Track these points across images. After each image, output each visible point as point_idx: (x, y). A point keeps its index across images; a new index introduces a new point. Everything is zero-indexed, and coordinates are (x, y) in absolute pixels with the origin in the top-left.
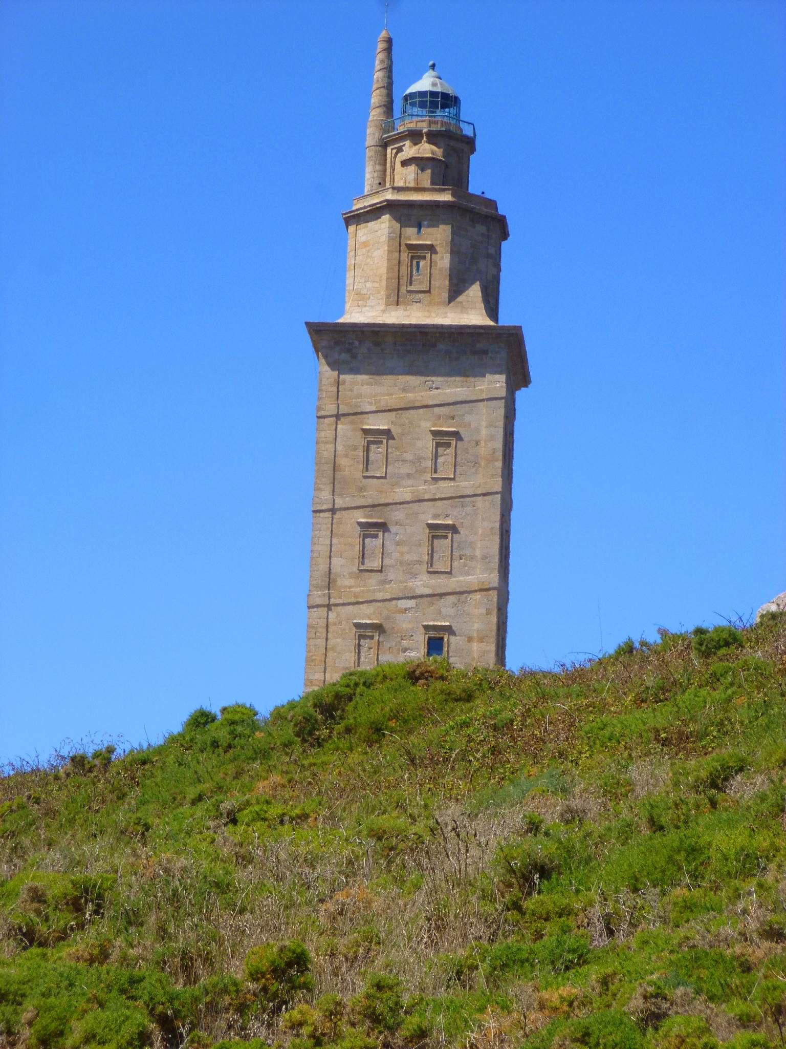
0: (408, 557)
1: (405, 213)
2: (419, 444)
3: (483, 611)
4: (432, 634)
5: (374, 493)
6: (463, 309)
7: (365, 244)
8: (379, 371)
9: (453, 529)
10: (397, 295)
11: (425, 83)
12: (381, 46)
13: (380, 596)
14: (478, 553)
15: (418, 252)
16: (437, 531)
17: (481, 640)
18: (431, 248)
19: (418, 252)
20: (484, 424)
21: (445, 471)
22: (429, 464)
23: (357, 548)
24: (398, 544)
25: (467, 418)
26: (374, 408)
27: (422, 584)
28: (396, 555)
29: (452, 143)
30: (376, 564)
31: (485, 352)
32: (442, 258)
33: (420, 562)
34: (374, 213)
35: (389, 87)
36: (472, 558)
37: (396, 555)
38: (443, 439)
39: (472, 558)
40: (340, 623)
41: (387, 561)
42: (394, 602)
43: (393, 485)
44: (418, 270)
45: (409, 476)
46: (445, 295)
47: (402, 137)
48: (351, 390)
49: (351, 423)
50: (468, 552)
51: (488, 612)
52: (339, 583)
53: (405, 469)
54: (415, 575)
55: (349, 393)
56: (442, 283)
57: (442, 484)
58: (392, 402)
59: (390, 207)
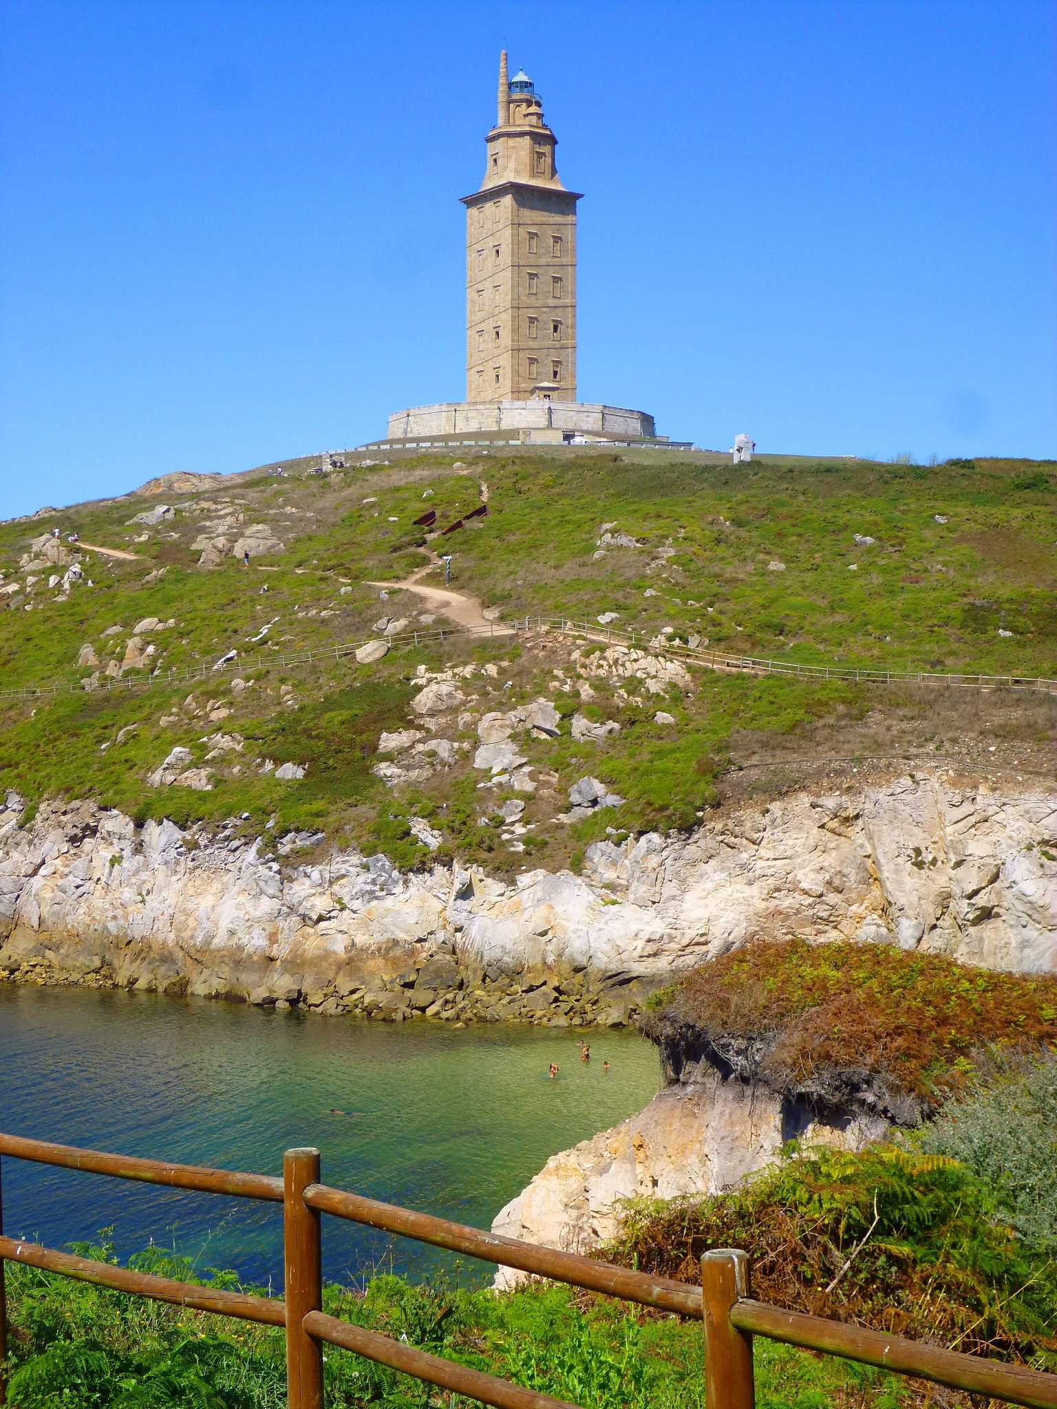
1: (537, 138)
5: (532, 261)
6: (556, 183)
7: (514, 148)
8: (532, 208)
9: (560, 279)
10: (534, 173)
11: (521, 77)
12: (503, 57)
15: (540, 155)
16: (556, 280)
18: (544, 154)
19: (540, 155)
27: (551, 302)
34: (522, 134)
38: (557, 239)
47: (522, 101)
53: (542, 251)
56: (548, 171)
59: (530, 134)
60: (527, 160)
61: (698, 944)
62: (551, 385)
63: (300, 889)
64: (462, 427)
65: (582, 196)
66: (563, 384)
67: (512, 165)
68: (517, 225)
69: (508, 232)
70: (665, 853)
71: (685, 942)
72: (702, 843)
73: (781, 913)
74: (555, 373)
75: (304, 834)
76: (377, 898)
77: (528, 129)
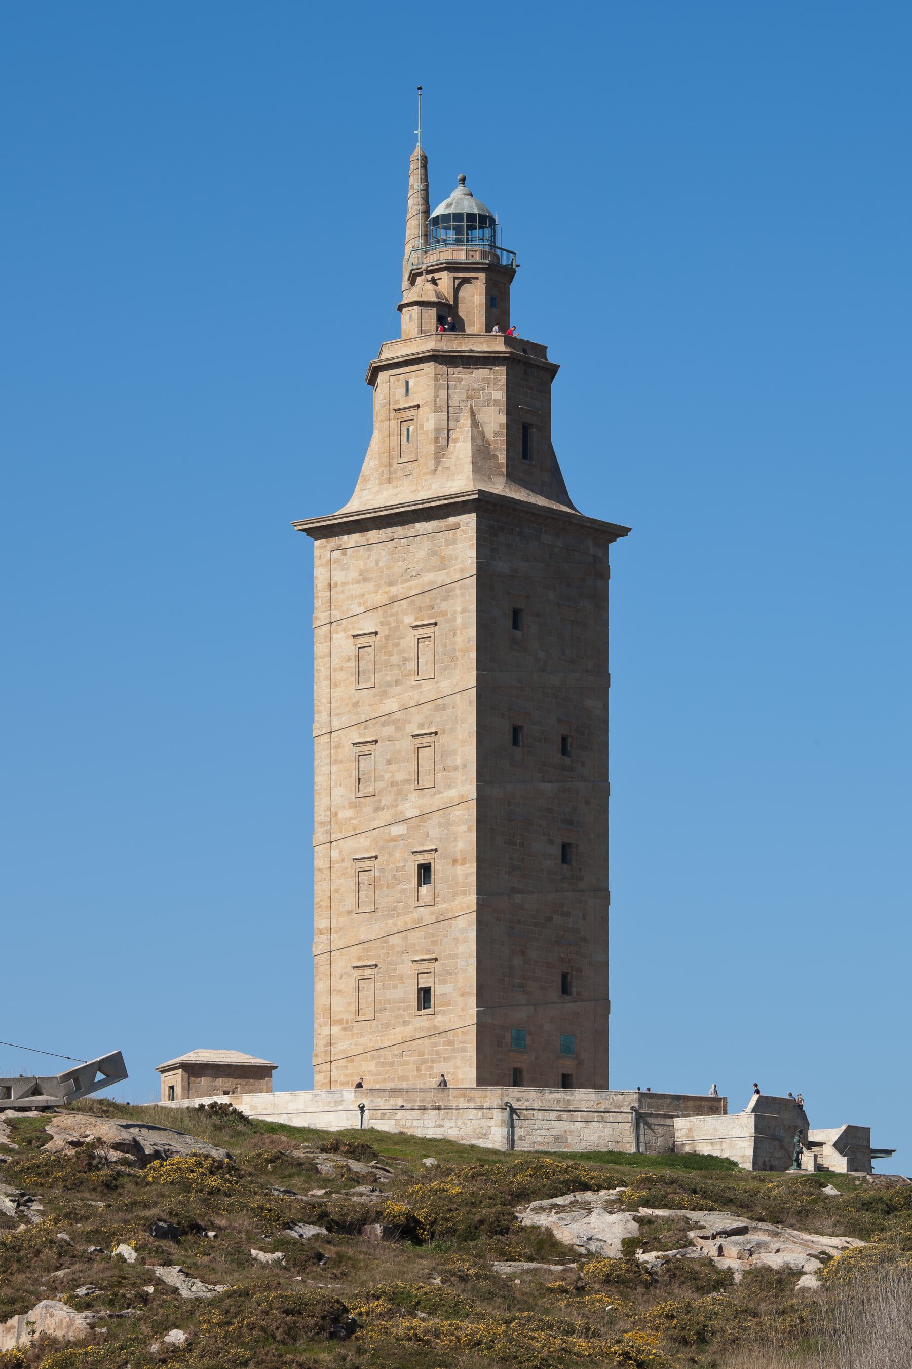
0: (400, 776)
2: (404, 643)
3: (465, 828)
4: (422, 859)
13: (375, 824)
14: (459, 762)
17: (464, 862)
20: (459, 609)
21: (426, 669)
22: (411, 665)
23: (355, 774)
24: (389, 762)
25: (444, 606)
26: (362, 609)
27: (411, 806)
28: (387, 776)
29: (461, 275)
30: (371, 790)
31: (456, 527)
32: (428, 420)
33: (408, 781)
35: (427, 212)
36: (455, 768)
37: (387, 776)
39: (455, 768)
40: (343, 860)
41: (380, 785)
42: (387, 829)
43: (384, 694)
44: (408, 440)
45: (397, 682)
46: (431, 464)
48: (343, 592)
49: (345, 630)
50: (449, 762)
51: (469, 830)
52: (340, 816)
54: (405, 798)
55: (342, 596)
57: (427, 686)
58: (379, 598)
66: (441, 1021)
74: (425, 996)
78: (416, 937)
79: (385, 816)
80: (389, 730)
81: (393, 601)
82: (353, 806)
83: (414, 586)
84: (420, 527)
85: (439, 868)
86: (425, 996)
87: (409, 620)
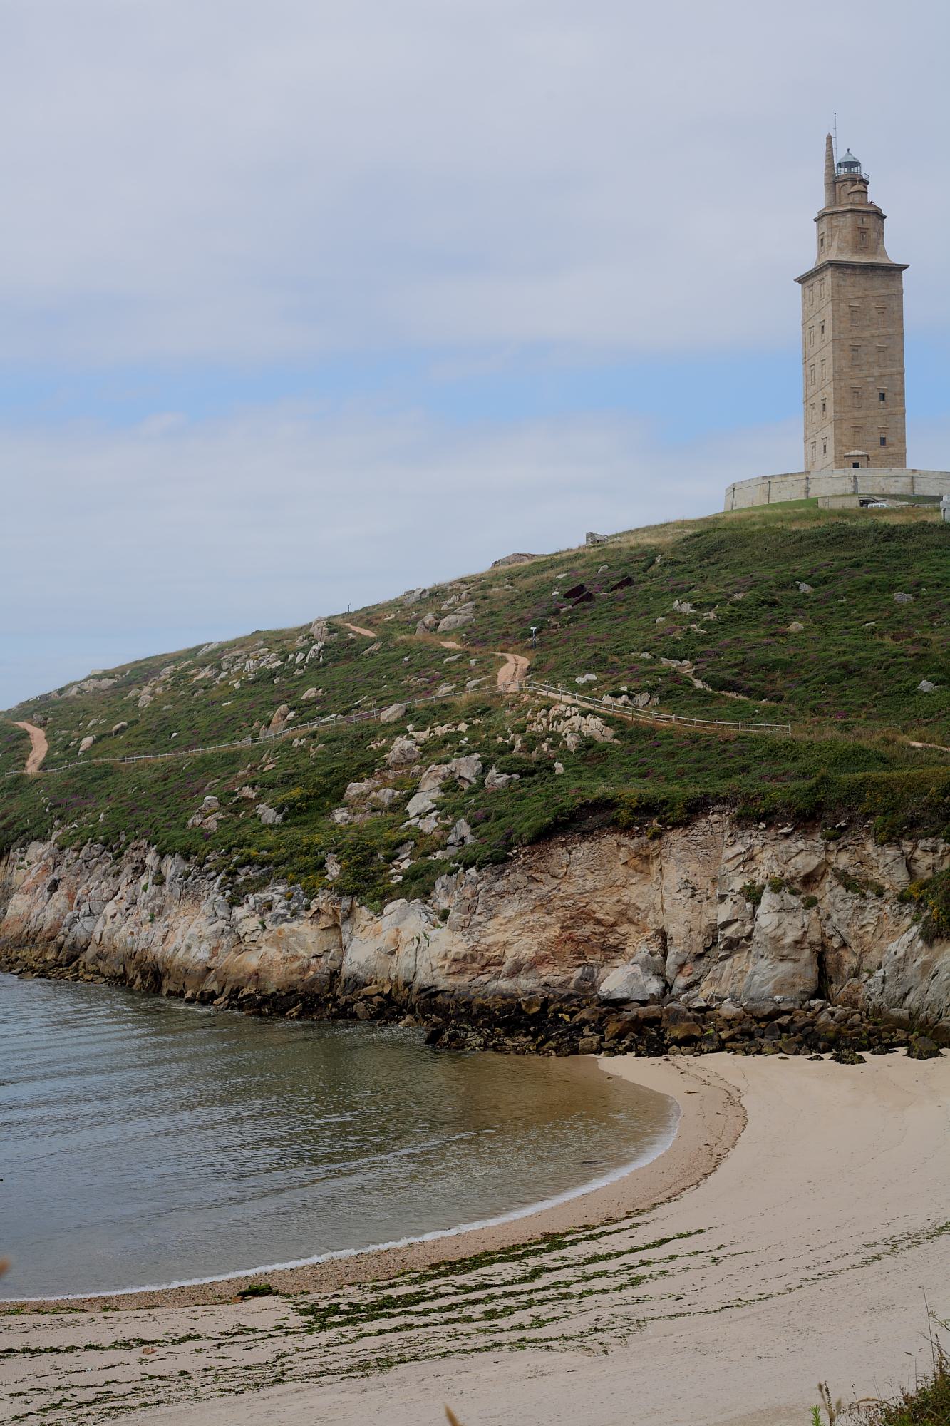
27: (876, 371)
58: (860, 294)
59: (851, 211)
60: (849, 237)
61: (493, 964)
62: (860, 453)
63: (239, 912)
64: (775, 499)
65: (905, 267)
67: (835, 243)
68: (837, 299)
69: (830, 307)
70: (479, 886)
71: (484, 962)
72: (511, 877)
73: (573, 940)
74: (883, 441)
75: (256, 867)
76: (286, 921)
77: (849, 207)
78: (879, 419)
79: (865, 373)
80: (865, 343)
81: (868, 296)
82: (851, 367)
83: (875, 293)
84: (878, 272)
85: (888, 395)
86: (883, 441)
87: (874, 304)
